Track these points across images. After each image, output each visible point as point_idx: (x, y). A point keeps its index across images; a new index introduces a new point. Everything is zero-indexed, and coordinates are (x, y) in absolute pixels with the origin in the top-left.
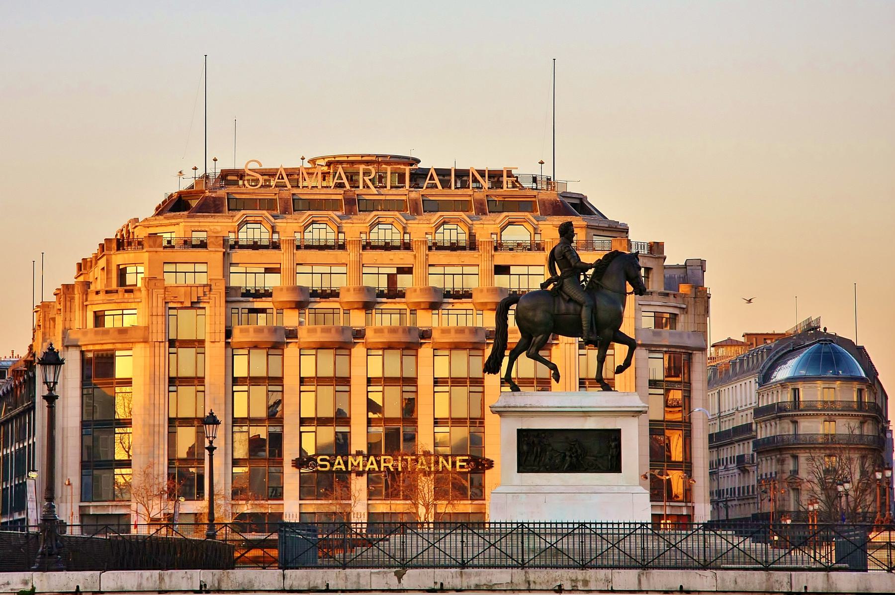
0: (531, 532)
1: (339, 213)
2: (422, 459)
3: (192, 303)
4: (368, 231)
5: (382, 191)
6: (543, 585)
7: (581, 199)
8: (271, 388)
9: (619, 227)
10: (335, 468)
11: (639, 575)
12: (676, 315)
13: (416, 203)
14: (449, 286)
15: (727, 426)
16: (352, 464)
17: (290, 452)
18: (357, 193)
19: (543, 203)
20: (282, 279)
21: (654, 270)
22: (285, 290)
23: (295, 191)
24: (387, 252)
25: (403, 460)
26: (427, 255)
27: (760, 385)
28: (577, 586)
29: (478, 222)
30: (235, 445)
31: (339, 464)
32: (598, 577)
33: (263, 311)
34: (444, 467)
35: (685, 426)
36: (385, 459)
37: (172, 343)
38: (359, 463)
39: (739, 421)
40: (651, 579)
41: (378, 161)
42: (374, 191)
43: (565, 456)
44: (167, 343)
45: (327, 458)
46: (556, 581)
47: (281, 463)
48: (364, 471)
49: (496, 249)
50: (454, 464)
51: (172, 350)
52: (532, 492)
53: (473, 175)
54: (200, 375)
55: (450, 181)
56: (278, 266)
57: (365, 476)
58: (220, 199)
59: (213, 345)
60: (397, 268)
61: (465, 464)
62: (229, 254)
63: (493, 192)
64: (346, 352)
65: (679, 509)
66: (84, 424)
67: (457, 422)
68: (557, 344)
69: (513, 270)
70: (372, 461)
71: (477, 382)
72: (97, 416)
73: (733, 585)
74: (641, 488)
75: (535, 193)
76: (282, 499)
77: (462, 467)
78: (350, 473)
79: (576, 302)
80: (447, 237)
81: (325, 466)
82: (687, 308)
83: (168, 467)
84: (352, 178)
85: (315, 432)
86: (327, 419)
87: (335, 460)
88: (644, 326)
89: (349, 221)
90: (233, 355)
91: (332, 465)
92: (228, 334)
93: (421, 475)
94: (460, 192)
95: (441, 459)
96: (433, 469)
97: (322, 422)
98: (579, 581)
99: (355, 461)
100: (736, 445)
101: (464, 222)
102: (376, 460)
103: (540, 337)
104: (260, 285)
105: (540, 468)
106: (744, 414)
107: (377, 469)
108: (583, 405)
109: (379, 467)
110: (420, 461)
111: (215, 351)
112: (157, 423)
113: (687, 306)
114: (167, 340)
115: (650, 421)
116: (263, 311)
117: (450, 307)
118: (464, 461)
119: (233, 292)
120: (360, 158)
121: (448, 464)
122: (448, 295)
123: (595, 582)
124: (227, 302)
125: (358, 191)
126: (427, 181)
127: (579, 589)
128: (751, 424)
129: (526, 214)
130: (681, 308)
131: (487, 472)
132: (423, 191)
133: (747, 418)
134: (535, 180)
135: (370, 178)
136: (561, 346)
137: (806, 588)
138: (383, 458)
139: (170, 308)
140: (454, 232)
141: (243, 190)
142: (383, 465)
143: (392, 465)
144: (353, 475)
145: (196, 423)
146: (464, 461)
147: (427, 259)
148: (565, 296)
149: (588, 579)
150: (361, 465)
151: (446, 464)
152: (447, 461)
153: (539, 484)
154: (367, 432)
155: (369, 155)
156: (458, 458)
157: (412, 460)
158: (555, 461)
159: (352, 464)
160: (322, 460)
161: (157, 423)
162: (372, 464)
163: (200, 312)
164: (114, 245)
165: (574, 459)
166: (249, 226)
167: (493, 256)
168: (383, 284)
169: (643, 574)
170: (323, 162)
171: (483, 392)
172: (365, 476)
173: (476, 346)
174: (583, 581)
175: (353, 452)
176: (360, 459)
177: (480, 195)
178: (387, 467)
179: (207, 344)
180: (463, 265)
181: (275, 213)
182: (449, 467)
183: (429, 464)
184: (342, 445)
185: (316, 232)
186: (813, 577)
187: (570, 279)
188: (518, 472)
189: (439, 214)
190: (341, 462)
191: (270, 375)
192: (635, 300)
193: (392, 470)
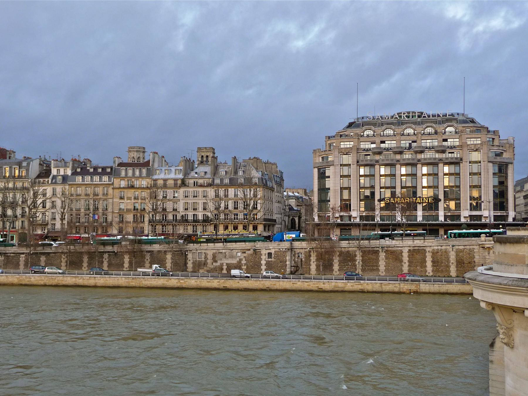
2: (418, 199)
5: (409, 119)
12: (503, 153)
17: (377, 197)
19: (460, 120)
20: (376, 146)
23: (382, 120)
30: (361, 195)
31: (392, 200)
33: (369, 155)
34: (425, 201)
37: (341, 165)
44: (339, 165)
47: (374, 200)
54: (349, 174)
58: (360, 124)
64: (395, 167)
66: (319, 189)
68: (462, 162)
69: (448, 140)
72: (322, 188)
77: (431, 201)
81: (388, 201)
83: (340, 202)
85: (385, 191)
86: (388, 187)
90: (359, 168)
91: (390, 201)
92: (358, 162)
93: (418, 204)
94: (433, 118)
111: (354, 167)
112: (336, 189)
116: (369, 155)
118: (432, 199)
119: (359, 150)
124: (357, 152)
125: (401, 119)
131: (439, 202)
139: (340, 155)
140: (430, 130)
145: (348, 189)
146: (432, 199)
152: (426, 199)
160: (387, 199)
161: (336, 189)
163: (349, 155)
164: (328, 138)
166: (367, 131)
167: (442, 136)
168: (408, 145)
171: (438, 178)
180: (432, 139)
183: (420, 200)
184: (393, 194)
192: (488, 148)
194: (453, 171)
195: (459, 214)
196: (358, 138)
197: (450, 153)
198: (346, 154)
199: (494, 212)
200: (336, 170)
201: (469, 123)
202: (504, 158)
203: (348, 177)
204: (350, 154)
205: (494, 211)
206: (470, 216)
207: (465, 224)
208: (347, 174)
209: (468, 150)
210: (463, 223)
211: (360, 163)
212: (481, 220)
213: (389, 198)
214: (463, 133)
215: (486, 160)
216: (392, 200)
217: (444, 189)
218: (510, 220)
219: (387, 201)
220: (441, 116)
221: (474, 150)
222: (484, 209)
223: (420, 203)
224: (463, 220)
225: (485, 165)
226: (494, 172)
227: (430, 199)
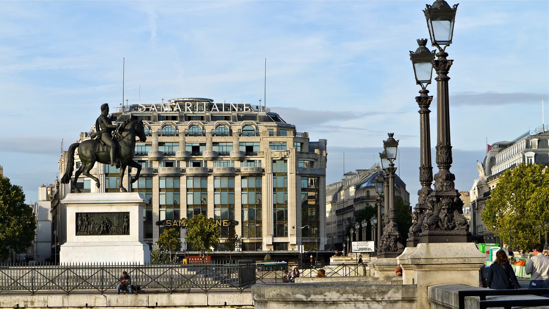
0: (37, 270)
1: (177, 122)
4: (188, 129)
5: (195, 112)
6: (8, 305)
7: (276, 115)
8: (147, 193)
9: (291, 126)
11: (63, 298)
12: (313, 162)
13: (208, 117)
14: (221, 151)
15: (346, 206)
16: (181, 223)
18: (184, 113)
19: (260, 117)
22: (153, 153)
23: (159, 113)
24: (195, 137)
26: (212, 138)
27: (356, 190)
28: (27, 305)
29: (233, 125)
31: (175, 223)
32: (39, 299)
35: (316, 207)
39: (349, 204)
40: (70, 300)
41: (194, 101)
42: (191, 112)
43: (100, 227)
45: (170, 221)
46: (15, 302)
48: (185, 226)
49: (240, 136)
50: (222, 223)
51: (107, 177)
52: (85, 245)
53: (232, 106)
55: (222, 108)
56: (151, 143)
60: (200, 144)
63: (240, 112)
67: (222, 206)
71: (232, 190)
73: (116, 303)
74: (140, 242)
75: (257, 113)
76: (152, 238)
77: (225, 224)
78: (180, 227)
79: (108, 146)
80: (220, 131)
81: (170, 224)
82: (317, 159)
84: (182, 107)
86: (170, 205)
87: (174, 222)
88: (300, 166)
89: (180, 125)
91: (172, 224)
95: (217, 221)
97: (167, 206)
98: (29, 302)
100: (348, 213)
101: (227, 124)
103: (90, 164)
104: (143, 150)
105: (87, 233)
106: (351, 201)
108: (109, 199)
117: (221, 159)
118: (226, 222)
120: (188, 99)
122: (220, 154)
123: (38, 302)
126: (213, 108)
127: (29, 306)
128: (353, 205)
129: (253, 121)
130: (315, 159)
132: (211, 112)
133: (351, 203)
134: (257, 107)
135: (190, 107)
136: (266, 175)
137: (157, 303)
140: (223, 129)
141: (138, 112)
144: (181, 228)
146: (226, 222)
148: (102, 143)
149: (34, 300)
152: (220, 222)
153: (87, 241)
154: (187, 210)
155: (192, 98)
156: (224, 221)
158: (95, 229)
160: (168, 222)
164: (84, 135)
165: (105, 228)
169: (65, 297)
170: (173, 101)
174: (31, 302)
175: (181, 219)
177: (234, 114)
181: (150, 121)
182: (220, 224)
185: (167, 129)
186: (161, 297)
187: (105, 133)
188: (76, 235)
189: (217, 121)
191: (147, 187)
194: (253, 185)
195: (260, 241)
199: (302, 239)
201: (273, 122)
202: (314, 170)
205: (302, 237)
207: (269, 253)
208: (115, 188)
210: (267, 252)
212: (287, 249)
214: (265, 135)
216: (175, 223)
217: (242, 208)
220: (237, 110)
222: (291, 235)
224: (265, 249)
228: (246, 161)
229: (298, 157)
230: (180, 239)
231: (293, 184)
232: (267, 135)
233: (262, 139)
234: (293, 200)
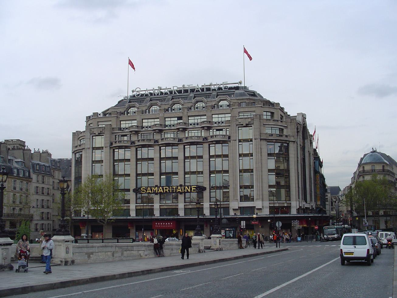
2: (179, 187)
3: (99, 133)
7: (254, 93)
10: (148, 192)
12: (283, 129)
16: (154, 190)
21: (275, 113)
23: (152, 97)
25: (172, 188)
26: (187, 112)
31: (149, 190)
34: (187, 190)
36: (165, 188)
38: (156, 190)
42: (178, 94)
44: (91, 149)
45: (145, 188)
57: (159, 195)
59: (105, 148)
61: (195, 189)
62: (119, 117)
65: (282, 204)
70: (179, 189)
71: (200, 157)
77: (193, 190)
81: (144, 191)
91: (146, 191)
92: (111, 144)
93: (179, 194)
95: (186, 187)
96: (183, 191)
99: (155, 189)
102: (162, 188)
107: (163, 192)
109: (163, 191)
110: (178, 188)
113: (287, 126)
114: (91, 147)
115: (268, 169)
121: (189, 189)
138: (165, 187)
142: (165, 190)
143: (168, 190)
147: (187, 114)
150: (157, 190)
151: (187, 188)
156: (193, 187)
157: (175, 188)
159: (154, 190)
160: (143, 189)
162: (161, 190)
167: (211, 111)
172: (159, 195)
173: (199, 143)
176: (157, 188)
178: (167, 191)
179: (104, 148)
182: (189, 190)
183: (182, 190)
190: (150, 189)
193: (168, 192)
195: (227, 206)
196: (117, 117)
197: (217, 130)
198: (97, 134)
199: (269, 203)
200: (87, 154)
203: (101, 162)
204: (103, 135)
206: (240, 208)
209: (237, 125)
211: (114, 145)
213: (145, 187)
214: (234, 106)
215: (258, 137)
216: (149, 190)
218: (294, 212)
219: (143, 191)
221: (244, 125)
223: (181, 193)
225: (257, 144)
226: (269, 152)
227: (193, 188)
228: (215, 130)
229: (264, 123)
230: (153, 204)
231: (257, 149)
232: (237, 106)
233: (233, 110)
234: (258, 164)
